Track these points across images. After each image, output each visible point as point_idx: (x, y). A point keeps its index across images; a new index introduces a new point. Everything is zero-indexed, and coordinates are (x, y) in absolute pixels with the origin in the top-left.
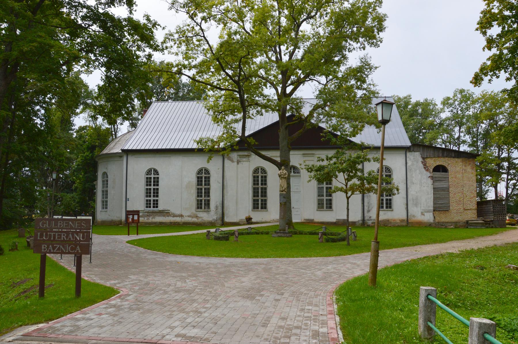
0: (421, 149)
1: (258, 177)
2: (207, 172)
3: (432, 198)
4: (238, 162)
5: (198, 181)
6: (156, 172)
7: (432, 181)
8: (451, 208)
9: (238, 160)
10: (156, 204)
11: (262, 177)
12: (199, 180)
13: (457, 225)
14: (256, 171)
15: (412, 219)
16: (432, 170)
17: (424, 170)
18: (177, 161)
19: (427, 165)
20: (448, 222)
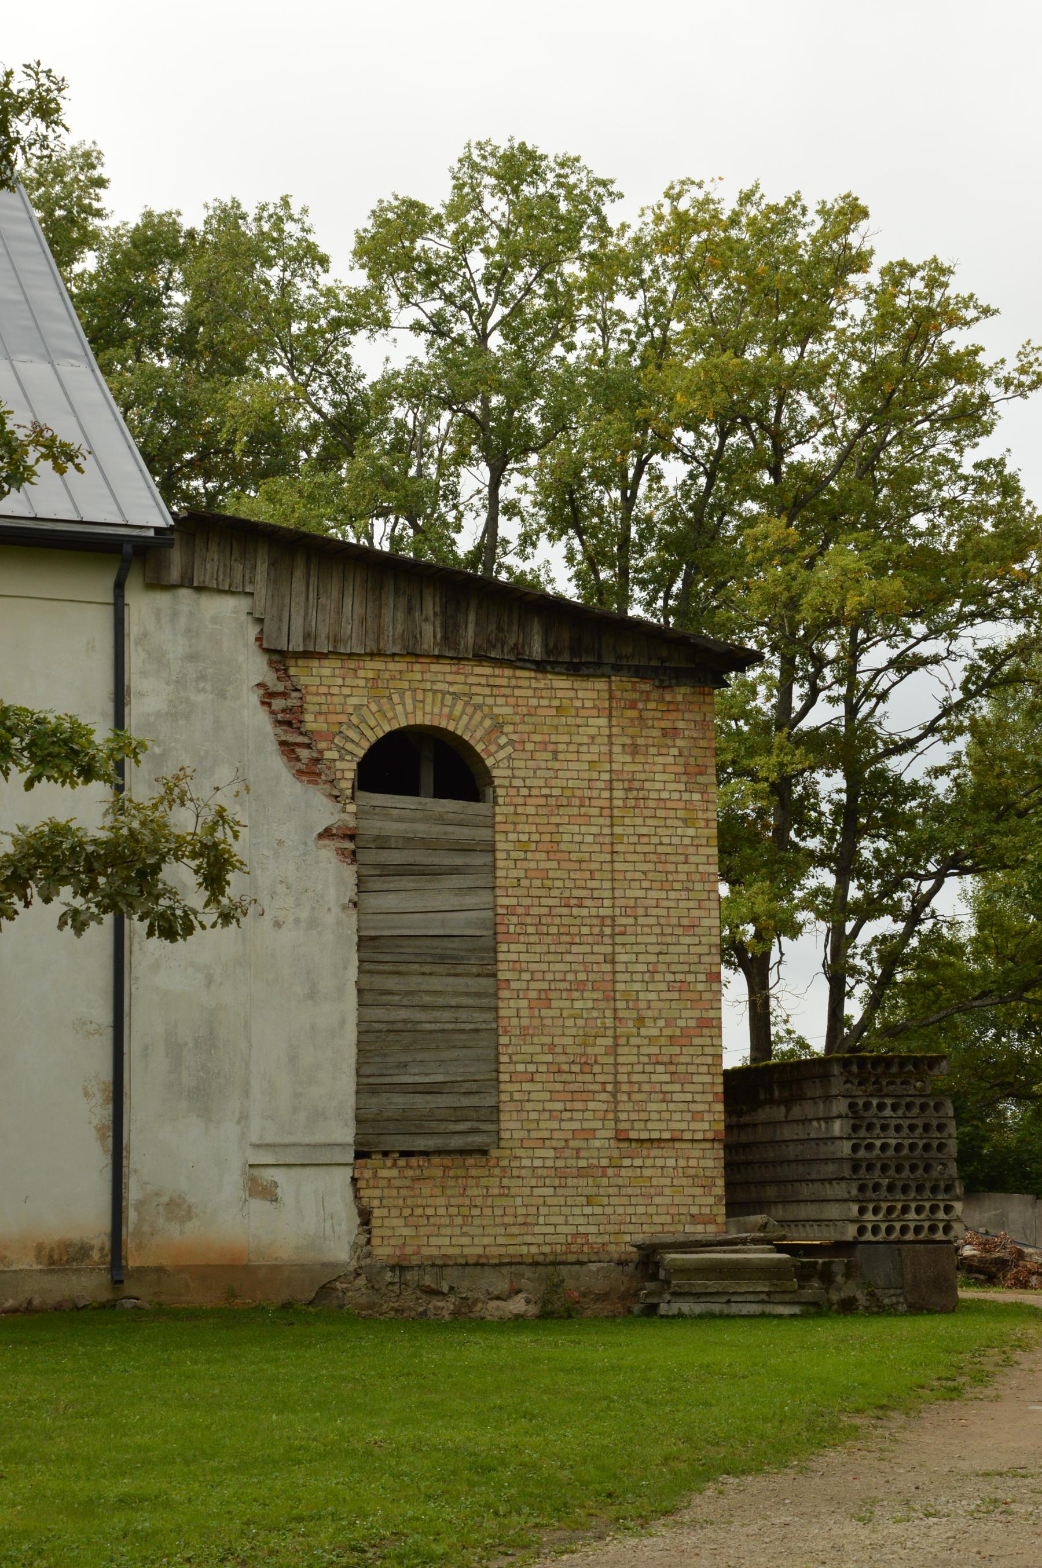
0: (262, 568)
3: (351, 1034)
7: (349, 873)
8: (510, 1125)
13: (555, 1287)
15: (155, 1242)
16: (348, 771)
17: (277, 763)
19: (311, 722)
20: (480, 1264)
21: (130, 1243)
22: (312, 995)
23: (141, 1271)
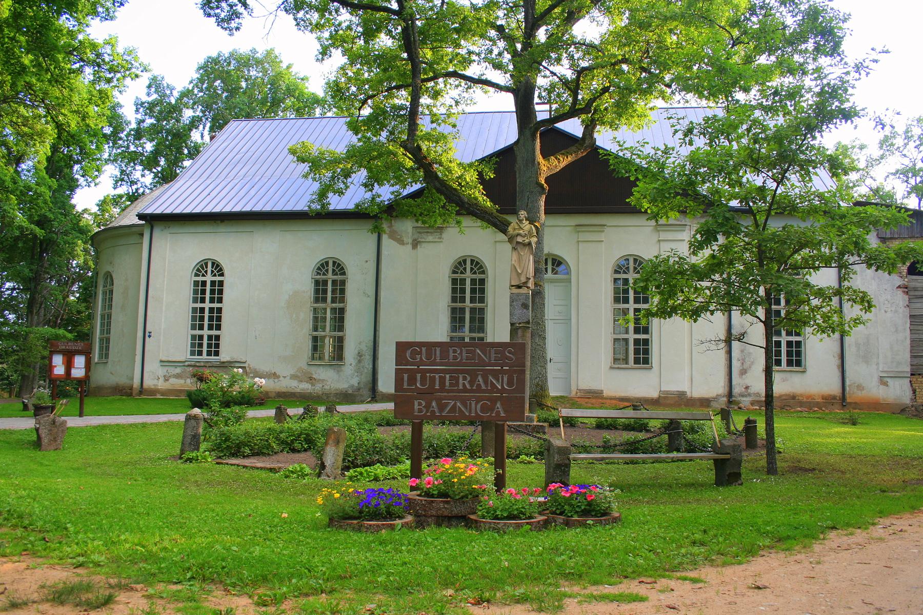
1: (463, 281)
2: (340, 268)
3: (908, 342)
4: (415, 244)
5: (317, 291)
6: (218, 269)
9: (414, 240)
10: (215, 345)
11: (473, 281)
12: (320, 288)
14: (460, 265)
15: (854, 395)
18: (267, 244)
21: (847, 396)
22: (896, 331)
23: (850, 403)
